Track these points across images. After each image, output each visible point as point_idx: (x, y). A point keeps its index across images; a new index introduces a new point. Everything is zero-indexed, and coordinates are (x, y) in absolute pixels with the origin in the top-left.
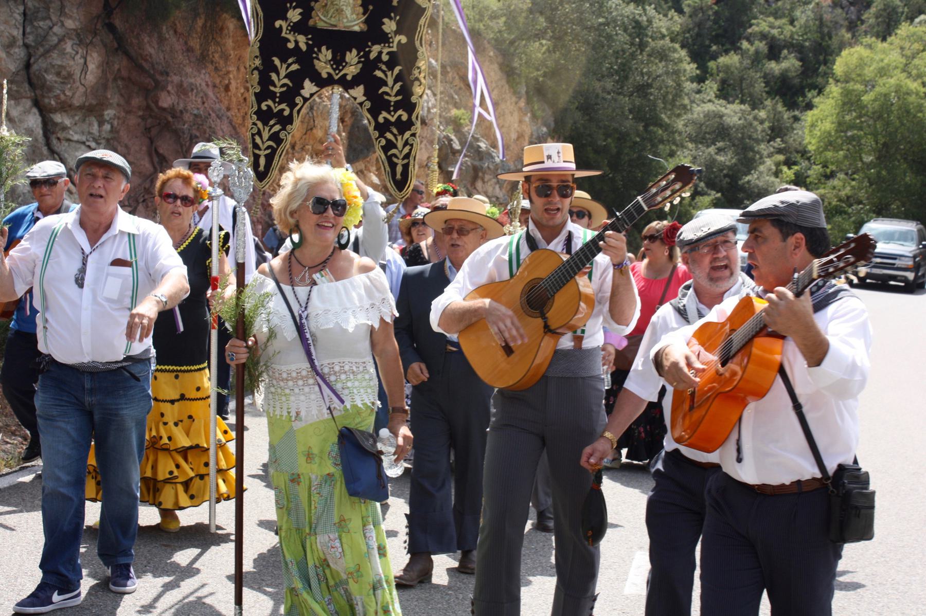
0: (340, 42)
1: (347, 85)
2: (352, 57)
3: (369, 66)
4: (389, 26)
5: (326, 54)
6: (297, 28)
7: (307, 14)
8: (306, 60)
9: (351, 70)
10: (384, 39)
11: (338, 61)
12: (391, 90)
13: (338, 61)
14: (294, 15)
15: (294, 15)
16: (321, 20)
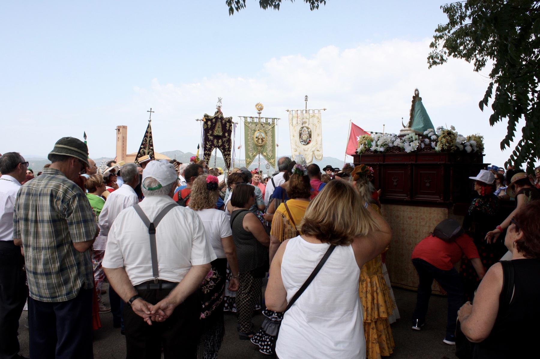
0: (218, 137)
1: (219, 147)
2: (220, 141)
3: (223, 143)
4: (226, 134)
5: (215, 141)
6: (211, 135)
7: (213, 132)
8: (212, 142)
9: (220, 144)
10: (225, 137)
11: (218, 142)
12: (227, 147)
13: (218, 142)
14: (210, 132)
15: (210, 132)
16: (216, 133)
